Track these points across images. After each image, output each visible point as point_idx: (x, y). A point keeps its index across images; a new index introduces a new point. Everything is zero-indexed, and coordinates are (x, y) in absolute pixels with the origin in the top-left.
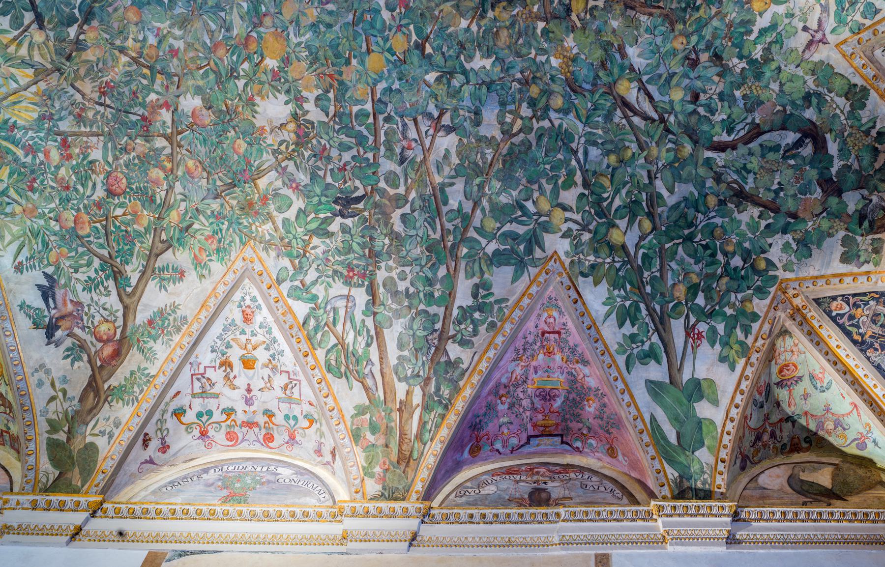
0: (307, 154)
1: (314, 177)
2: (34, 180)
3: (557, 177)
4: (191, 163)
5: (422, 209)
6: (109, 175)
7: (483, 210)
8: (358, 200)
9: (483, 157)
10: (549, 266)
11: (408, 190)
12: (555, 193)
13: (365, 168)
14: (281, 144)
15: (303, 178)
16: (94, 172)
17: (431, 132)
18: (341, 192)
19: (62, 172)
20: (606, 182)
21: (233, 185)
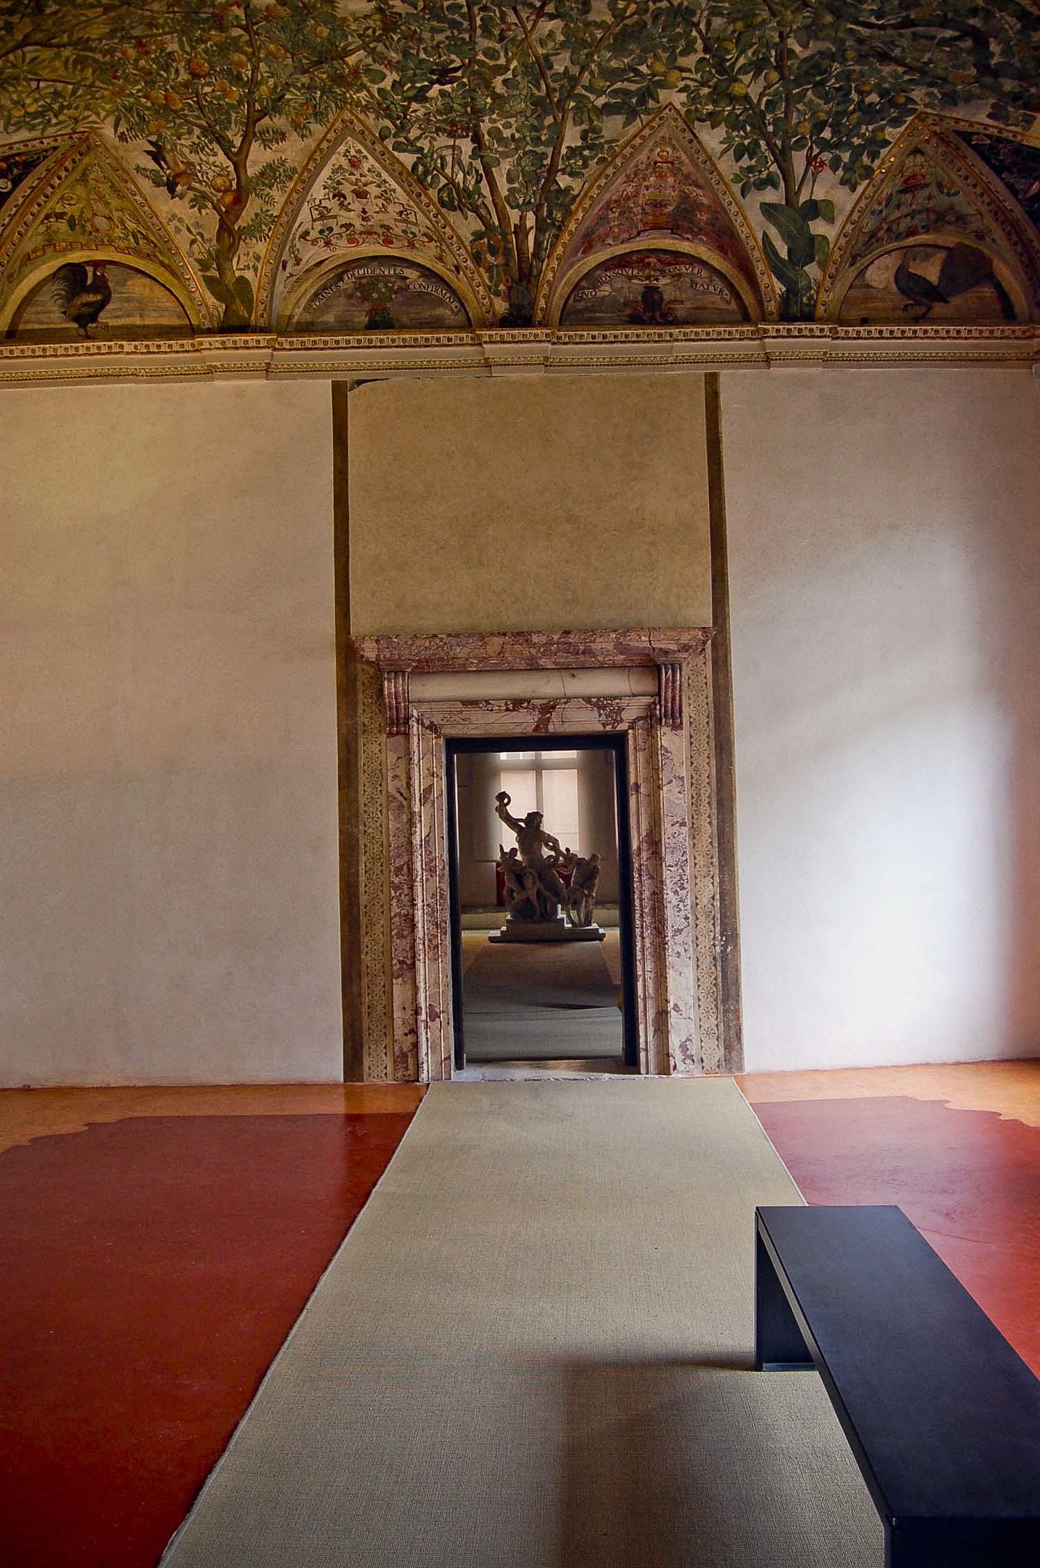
0: (396, 38)
1: (405, 54)
2: (116, 71)
3: (674, 48)
4: (272, 47)
5: (525, 74)
6: (189, 62)
7: (592, 73)
8: (456, 70)
9: (592, 35)
10: (663, 114)
11: (509, 61)
12: (673, 58)
13: (464, 47)
14: (367, 29)
15: (394, 56)
16: (174, 61)
17: (533, 17)
18: (437, 64)
19: (142, 62)
20: (730, 46)
21: (320, 62)
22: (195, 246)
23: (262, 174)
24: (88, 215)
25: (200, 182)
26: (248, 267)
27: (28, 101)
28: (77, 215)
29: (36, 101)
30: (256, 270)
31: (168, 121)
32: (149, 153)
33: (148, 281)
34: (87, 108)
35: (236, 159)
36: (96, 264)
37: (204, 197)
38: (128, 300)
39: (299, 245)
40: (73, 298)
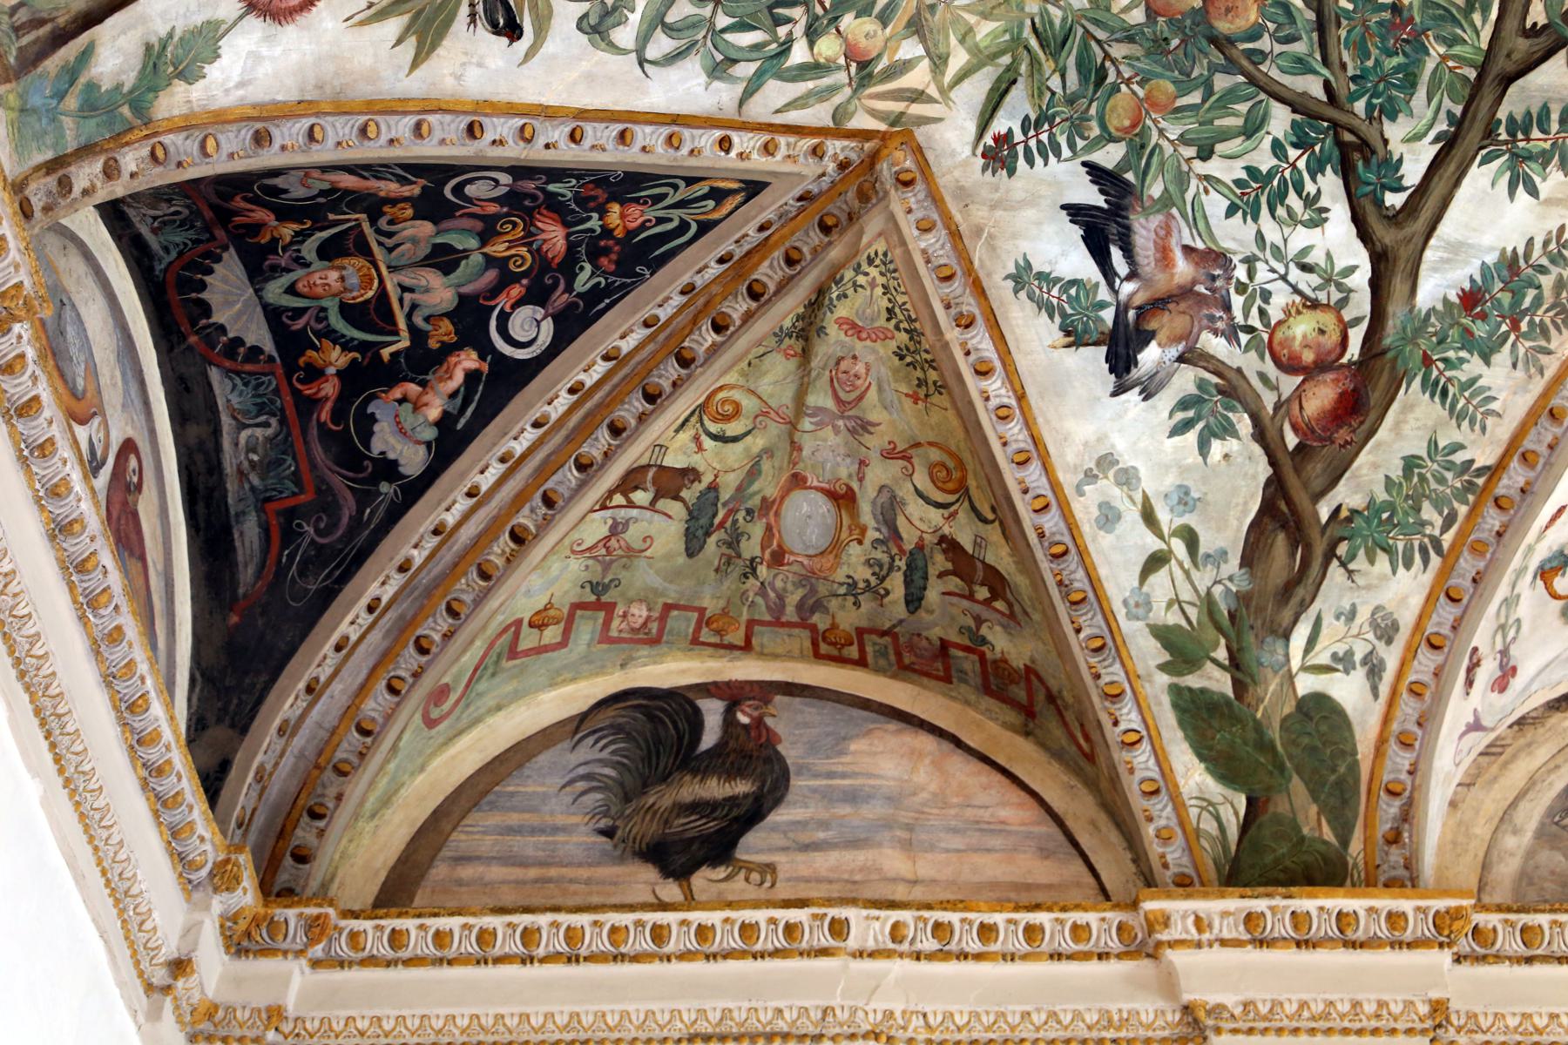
22: (1160, 579)
23: (1471, 299)
24: (768, 486)
25: (1231, 334)
26: (1344, 662)
28: (729, 484)
30: (1374, 670)
31: (1184, 88)
32: (1076, 212)
33: (926, 742)
34: (916, 27)
35: (1385, 235)
36: (733, 694)
37: (1231, 388)
38: (853, 797)
39: (1531, 597)
40: (645, 786)
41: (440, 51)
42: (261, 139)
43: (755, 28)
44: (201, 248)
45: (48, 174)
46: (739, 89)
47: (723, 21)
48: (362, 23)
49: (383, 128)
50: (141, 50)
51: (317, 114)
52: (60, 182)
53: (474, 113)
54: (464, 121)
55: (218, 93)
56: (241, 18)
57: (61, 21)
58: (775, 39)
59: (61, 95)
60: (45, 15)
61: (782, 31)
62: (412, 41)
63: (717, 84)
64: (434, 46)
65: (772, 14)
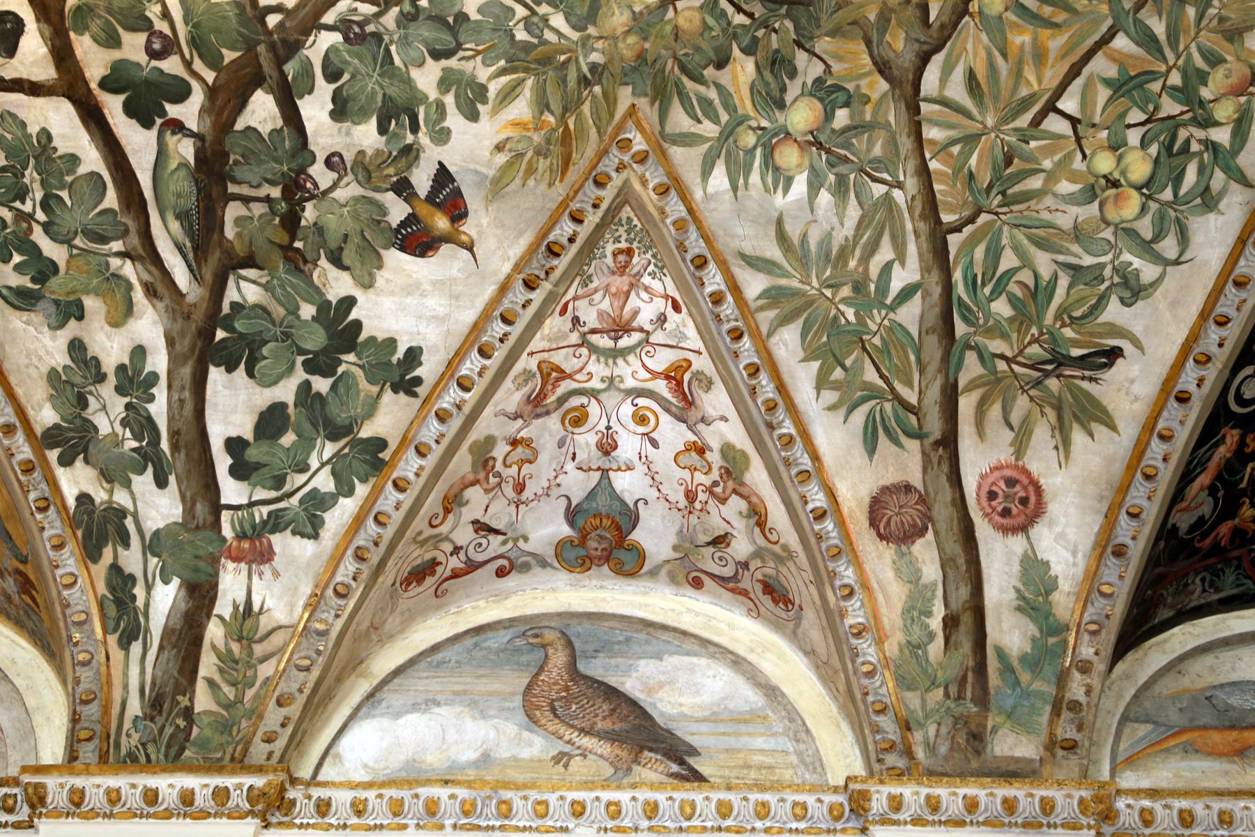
27: (1105, 163)
29: (1116, 146)
41: (1110, 408)
42: (1120, 552)
43: (1184, 170)
44: (1245, 564)
45: (1059, 715)
46: (1234, 186)
47: (1167, 195)
48: (1067, 457)
49: (1152, 462)
50: (1018, 614)
51: (1120, 506)
52: (1069, 709)
53: (1169, 394)
54: (1172, 403)
55: (1073, 570)
56: (1028, 538)
57: (971, 663)
58: (1200, 153)
59: (1017, 683)
60: (961, 673)
61: (1195, 147)
62: (1095, 426)
63: (1222, 206)
64: (1105, 411)
65: (1178, 154)
